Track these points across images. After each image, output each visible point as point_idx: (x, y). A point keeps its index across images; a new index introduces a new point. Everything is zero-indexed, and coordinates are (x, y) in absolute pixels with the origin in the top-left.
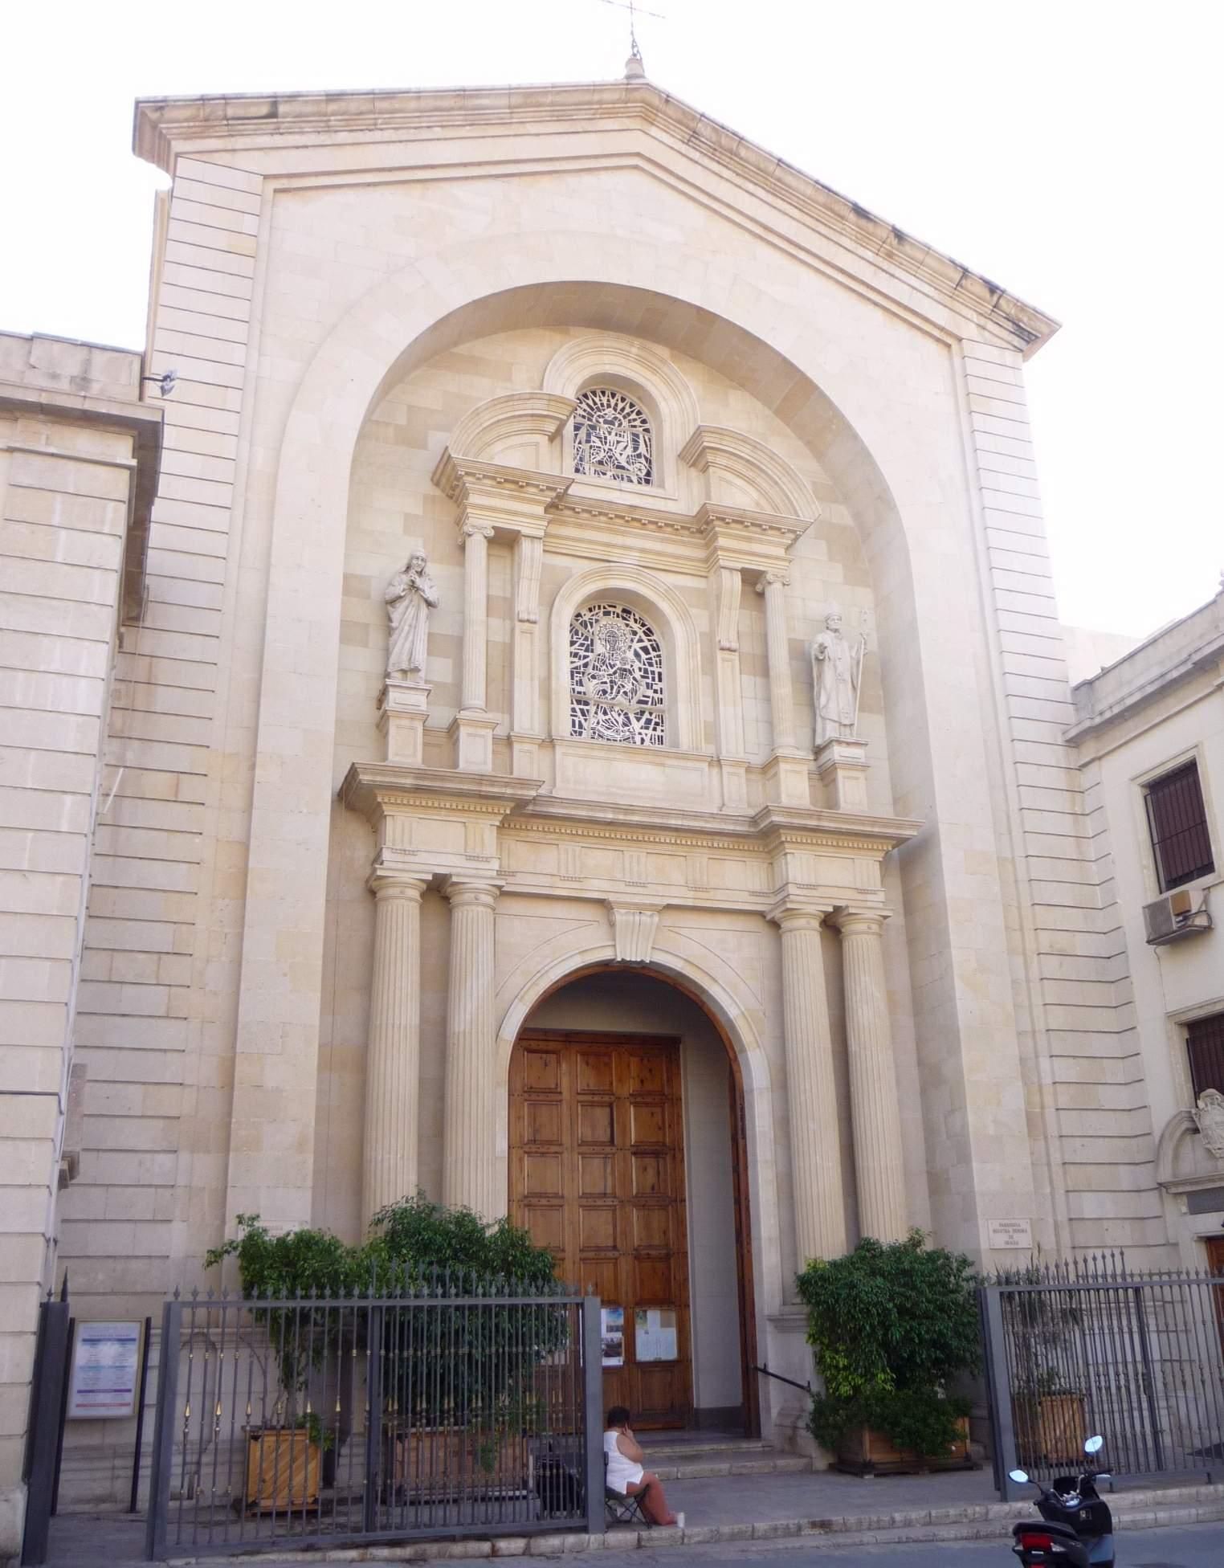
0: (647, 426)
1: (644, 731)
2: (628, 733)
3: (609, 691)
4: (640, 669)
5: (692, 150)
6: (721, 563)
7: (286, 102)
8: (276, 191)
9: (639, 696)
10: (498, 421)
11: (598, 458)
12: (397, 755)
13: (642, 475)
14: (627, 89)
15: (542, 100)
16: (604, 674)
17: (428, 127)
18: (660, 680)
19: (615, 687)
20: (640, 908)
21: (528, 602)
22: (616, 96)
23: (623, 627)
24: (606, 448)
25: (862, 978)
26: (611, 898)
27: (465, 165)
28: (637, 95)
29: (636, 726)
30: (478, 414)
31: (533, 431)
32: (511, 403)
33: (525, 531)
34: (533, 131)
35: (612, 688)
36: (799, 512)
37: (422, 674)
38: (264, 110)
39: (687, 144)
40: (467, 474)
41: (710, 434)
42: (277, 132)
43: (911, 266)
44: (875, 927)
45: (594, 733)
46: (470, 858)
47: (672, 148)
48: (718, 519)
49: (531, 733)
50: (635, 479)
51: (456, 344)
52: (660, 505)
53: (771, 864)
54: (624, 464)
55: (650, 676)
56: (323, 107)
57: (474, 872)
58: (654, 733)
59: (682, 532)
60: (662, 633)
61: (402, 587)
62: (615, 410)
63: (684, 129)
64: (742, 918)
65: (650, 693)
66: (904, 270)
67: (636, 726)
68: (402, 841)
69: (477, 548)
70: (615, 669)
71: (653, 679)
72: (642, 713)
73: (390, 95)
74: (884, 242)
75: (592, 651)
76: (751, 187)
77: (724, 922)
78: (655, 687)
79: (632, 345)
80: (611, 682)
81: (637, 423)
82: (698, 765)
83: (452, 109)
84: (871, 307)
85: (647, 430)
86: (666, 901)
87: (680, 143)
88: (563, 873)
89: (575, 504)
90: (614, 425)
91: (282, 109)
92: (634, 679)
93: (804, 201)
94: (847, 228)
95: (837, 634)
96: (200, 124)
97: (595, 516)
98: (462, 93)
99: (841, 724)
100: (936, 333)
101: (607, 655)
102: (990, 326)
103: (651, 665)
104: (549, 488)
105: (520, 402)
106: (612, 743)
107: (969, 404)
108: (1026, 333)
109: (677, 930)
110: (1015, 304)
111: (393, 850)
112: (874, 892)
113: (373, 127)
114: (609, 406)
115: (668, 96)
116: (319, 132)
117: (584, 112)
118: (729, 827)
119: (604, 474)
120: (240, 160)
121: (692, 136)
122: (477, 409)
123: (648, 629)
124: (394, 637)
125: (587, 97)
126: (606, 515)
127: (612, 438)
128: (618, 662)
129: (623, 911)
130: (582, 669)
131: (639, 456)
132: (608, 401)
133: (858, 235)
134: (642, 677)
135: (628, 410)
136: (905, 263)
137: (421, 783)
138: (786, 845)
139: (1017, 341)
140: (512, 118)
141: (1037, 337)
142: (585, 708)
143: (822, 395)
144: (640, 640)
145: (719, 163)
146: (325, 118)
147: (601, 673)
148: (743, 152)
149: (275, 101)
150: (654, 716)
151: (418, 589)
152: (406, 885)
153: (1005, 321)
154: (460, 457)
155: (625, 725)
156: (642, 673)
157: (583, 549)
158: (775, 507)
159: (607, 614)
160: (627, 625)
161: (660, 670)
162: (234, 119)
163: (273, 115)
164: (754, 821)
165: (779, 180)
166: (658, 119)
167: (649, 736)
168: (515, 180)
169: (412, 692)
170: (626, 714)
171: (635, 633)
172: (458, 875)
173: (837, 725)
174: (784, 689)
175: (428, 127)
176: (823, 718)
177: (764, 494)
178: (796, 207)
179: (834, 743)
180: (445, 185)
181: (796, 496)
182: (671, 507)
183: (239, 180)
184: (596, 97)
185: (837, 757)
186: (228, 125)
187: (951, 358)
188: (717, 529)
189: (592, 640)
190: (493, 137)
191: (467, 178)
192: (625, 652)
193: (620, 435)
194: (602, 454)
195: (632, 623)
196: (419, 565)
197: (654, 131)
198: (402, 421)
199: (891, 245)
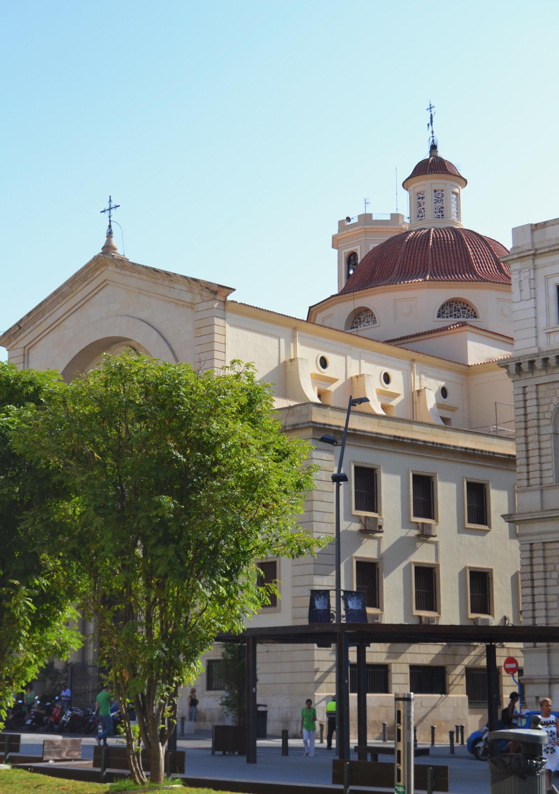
8: (28, 350)
22: (94, 264)
27: (66, 313)
38: (18, 328)
42: (24, 331)
91: (21, 325)
98: (55, 293)
125: (87, 270)
149: (18, 324)
168: (79, 310)
180: (63, 323)
184: (89, 269)
191: (68, 317)
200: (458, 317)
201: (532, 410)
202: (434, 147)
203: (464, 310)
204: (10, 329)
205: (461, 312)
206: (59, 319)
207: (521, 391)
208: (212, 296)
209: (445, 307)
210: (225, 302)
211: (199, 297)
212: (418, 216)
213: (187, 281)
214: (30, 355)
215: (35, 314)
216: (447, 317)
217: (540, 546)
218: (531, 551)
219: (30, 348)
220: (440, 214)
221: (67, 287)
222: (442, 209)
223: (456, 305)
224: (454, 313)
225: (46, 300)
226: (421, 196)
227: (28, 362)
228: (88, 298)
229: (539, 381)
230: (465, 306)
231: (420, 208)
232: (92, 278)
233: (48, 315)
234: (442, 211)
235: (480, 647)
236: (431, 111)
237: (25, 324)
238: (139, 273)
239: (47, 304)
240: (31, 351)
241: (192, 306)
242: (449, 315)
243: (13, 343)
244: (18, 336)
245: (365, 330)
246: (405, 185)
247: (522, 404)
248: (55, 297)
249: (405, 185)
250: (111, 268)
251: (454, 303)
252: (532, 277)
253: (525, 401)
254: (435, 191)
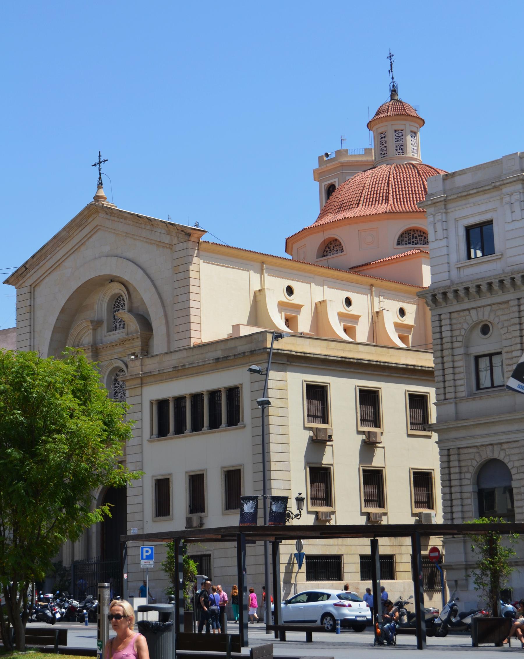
8: (34, 288)
22: (87, 212)
38: (24, 269)
73: (42, 248)
80: (123, 393)
83: (56, 242)
91: (27, 266)
98: (55, 237)
149: (24, 266)
191: (66, 258)
200: (416, 244)
201: (446, 334)
202: (394, 91)
203: (420, 237)
205: (418, 239)
206: (59, 260)
207: (437, 318)
208: (187, 238)
209: (404, 236)
210: (198, 243)
211: (176, 238)
212: (381, 154)
213: (165, 225)
214: (36, 293)
216: (406, 244)
217: (456, 451)
218: (449, 455)
219: (36, 286)
220: (400, 151)
221: (65, 232)
222: (402, 147)
223: (413, 233)
224: (412, 240)
225: (47, 244)
226: (383, 136)
227: (34, 298)
228: (83, 241)
229: (452, 309)
230: (422, 234)
231: (382, 146)
234: (402, 149)
235: (367, 541)
236: (391, 59)
237: (30, 265)
238: (126, 218)
239: (49, 247)
240: (36, 289)
241: (171, 247)
242: (407, 243)
244: (25, 276)
245: (334, 258)
246: (369, 126)
247: (438, 329)
249: (369, 125)
250: (102, 215)
251: (411, 232)
252: (444, 220)
253: (441, 326)
254: (396, 131)
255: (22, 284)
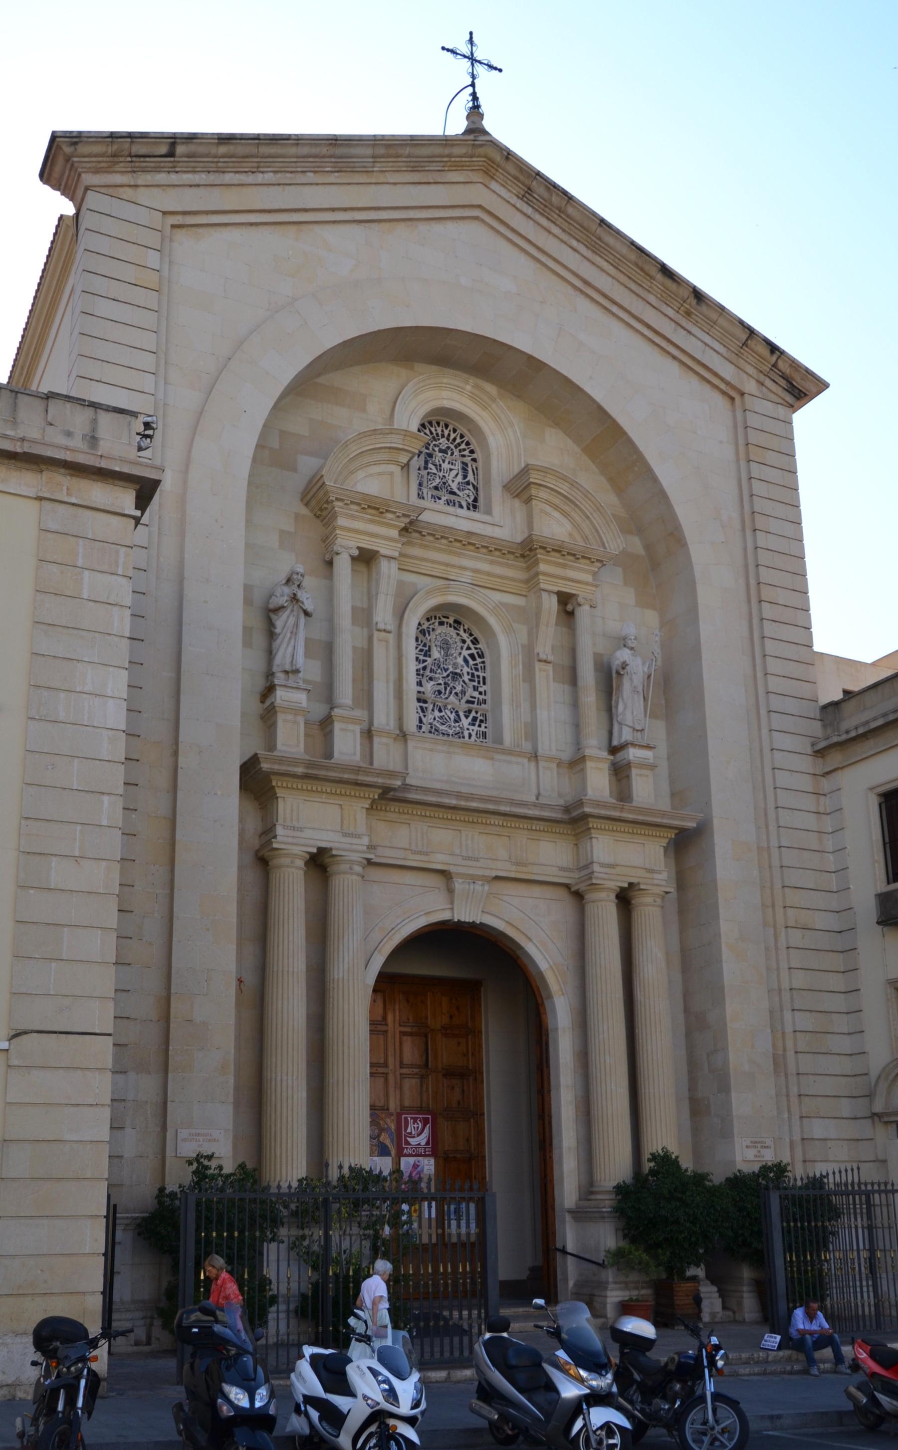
0: (474, 456)
1: (471, 727)
2: (458, 729)
3: (443, 692)
4: (468, 673)
5: (525, 205)
6: (542, 586)
7: (183, 143)
8: (173, 226)
9: (467, 697)
10: (362, 452)
11: (434, 484)
12: (283, 745)
13: (470, 501)
14: (474, 144)
15: (401, 151)
16: (440, 676)
17: (303, 172)
18: (484, 683)
19: (448, 689)
20: (474, 879)
21: (383, 615)
22: (463, 150)
23: (455, 636)
24: (441, 474)
25: (648, 942)
26: (452, 869)
27: (333, 210)
28: (481, 151)
29: (465, 722)
30: (347, 446)
31: (389, 462)
32: (373, 437)
33: (383, 551)
34: (392, 181)
35: (446, 689)
36: (606, 545)
37: (301, 675)
38: (164, 150)
39: (521, 199)
40: (337, 499)
41: (536, 472)
43: (705, 325)
44: (659, 901)
45: (432, 727)
46: (345, 835)
47: (508, 202)
48: (541, 547)
49: (388, 728)
50: (464, 504)
51: (319, 375)
52: (488, 531)
53: (576, 845)
54: (454, 487)
55: (476, 679)
56: (213, 150)
57: (348, 846)
58: (479, 729)
59: (508, 556)
60: (487, 643)
61: (286, 598)
62: (448, 440)
63: (521, 185)
64: (551, 888)
65: (476, 694)
66: (699, 328)
67: (465, 722)
68: (292, 819)
69: (343, 565)
70: (448, 672)
71: (479, 682)
72: (470, 711)
74: (684, 302)
75: (430, 656)
76: (574, 243)
77: (537, 890)
78: (480, 689)
79: (467, 383)
80: (445, 683)
81: (466, 453)
82: (520, 760)
83: (324, 157)
84: (670, 360)
85: (474, 460)
86: (494, 874)
87: (515, 198)
88: (413, 847)
89: (423, 528)
90: (447, 454)
91: (180, 149)
92: (464, 681)
93: (619, 259)
94: (654, 287)
95: (633, 652)
96: (108, 159)
97: (437, 539)
98: (334, 141)
99: (634, 729)
100: (723, 386)
101: (442, 660)
102: (768, 383)
103: (477, 670)
104: (404, 515)
105: (381, 436)
106: (445, 738)
107: (747, 453)
108: (797, 391)
109: (500, 897)
110: (791, 365)
111: (285, 827)
112: (659, 872)
113: (255, 170)
114: (443, 436)
115: (509, 154)
116: (209, 172)
117: (434, 164)
118: (546, 814)
119: (440, 499)
120: (143, 196)
121: (526, 192)
122: (346, 442)
123: (475, 639)
124: (278, 641)
125: (438, 150)
126: (447, 538)
127: (445, 466)
128: (450, 667)
129: (460, 881)
130: (422, 672)
131: (468, 483)
132: (442, 431)
133: (664, 294)
134: (470, 680)
135: (458, 440)
136: (699, 320)
137: (310, 771)
138: (593, 831)
139: (789, 399)
140: (373, 167)
141: (806, 395)
142: (424, 705)
143: (630, 441)
144: (469, 648)
145: (548, 218)
146: (216, 160)
147: (437, 676)
148: (570, 210)
149: (174, 140)
150: (478, 715)
151: (298, 601)
152: (295, 856)
153: (781, 379)
154: (332, 484)
155: (456, 721)
156: (470, 677)
157: (426, 567)
158: (585, 538)
159: (441, 623)
160: (458, 634)
161: (484, 675)
162: (136, 156)
163: (171, 154)
164: (567, 809)
165: (600, 239)
166: (498, 174)
167: (475, 731)
168: (375, 226)
169: (294, 691)
170: (457, 712)
171: (464, 642)
172: (338, 849)
173: (631, 730)
174: (590, 698)
175: (303, 172)
176: (620, 724)
177: (577, 527)
178: (612, 265)
179: (629, 746)
180: (316, 228)
181: (605, 531)
182: (497, 533)
183: (144, 217)
184: (447, 151)
185: (631, 757)
186: (131, 162)
187: (734, 411)
188: (539, 556)
189: (430, 647)
190: (357, 184)
191: (334, 222)
192: (456, 658)
193: (452, 464)
194: (438, 480)
195: (462, 632)
196: (298, 580)
197: (494, 185)
198: (276, 445)
199: (690, 305)
204: (144, 136)
206: (306, 210)
215: (240, 150)
221: (369, 151)
232: (438, 177)
233: (269, 177)
239: (293, 150)
243: (118, 179)
244: (144, 171)
248: (324, 151)
255: (121, 186)
